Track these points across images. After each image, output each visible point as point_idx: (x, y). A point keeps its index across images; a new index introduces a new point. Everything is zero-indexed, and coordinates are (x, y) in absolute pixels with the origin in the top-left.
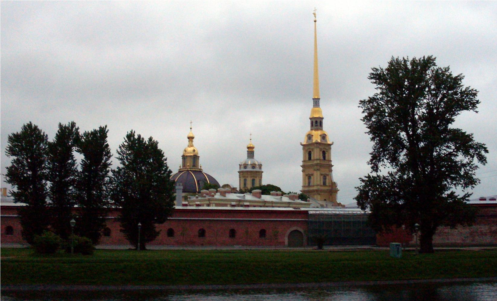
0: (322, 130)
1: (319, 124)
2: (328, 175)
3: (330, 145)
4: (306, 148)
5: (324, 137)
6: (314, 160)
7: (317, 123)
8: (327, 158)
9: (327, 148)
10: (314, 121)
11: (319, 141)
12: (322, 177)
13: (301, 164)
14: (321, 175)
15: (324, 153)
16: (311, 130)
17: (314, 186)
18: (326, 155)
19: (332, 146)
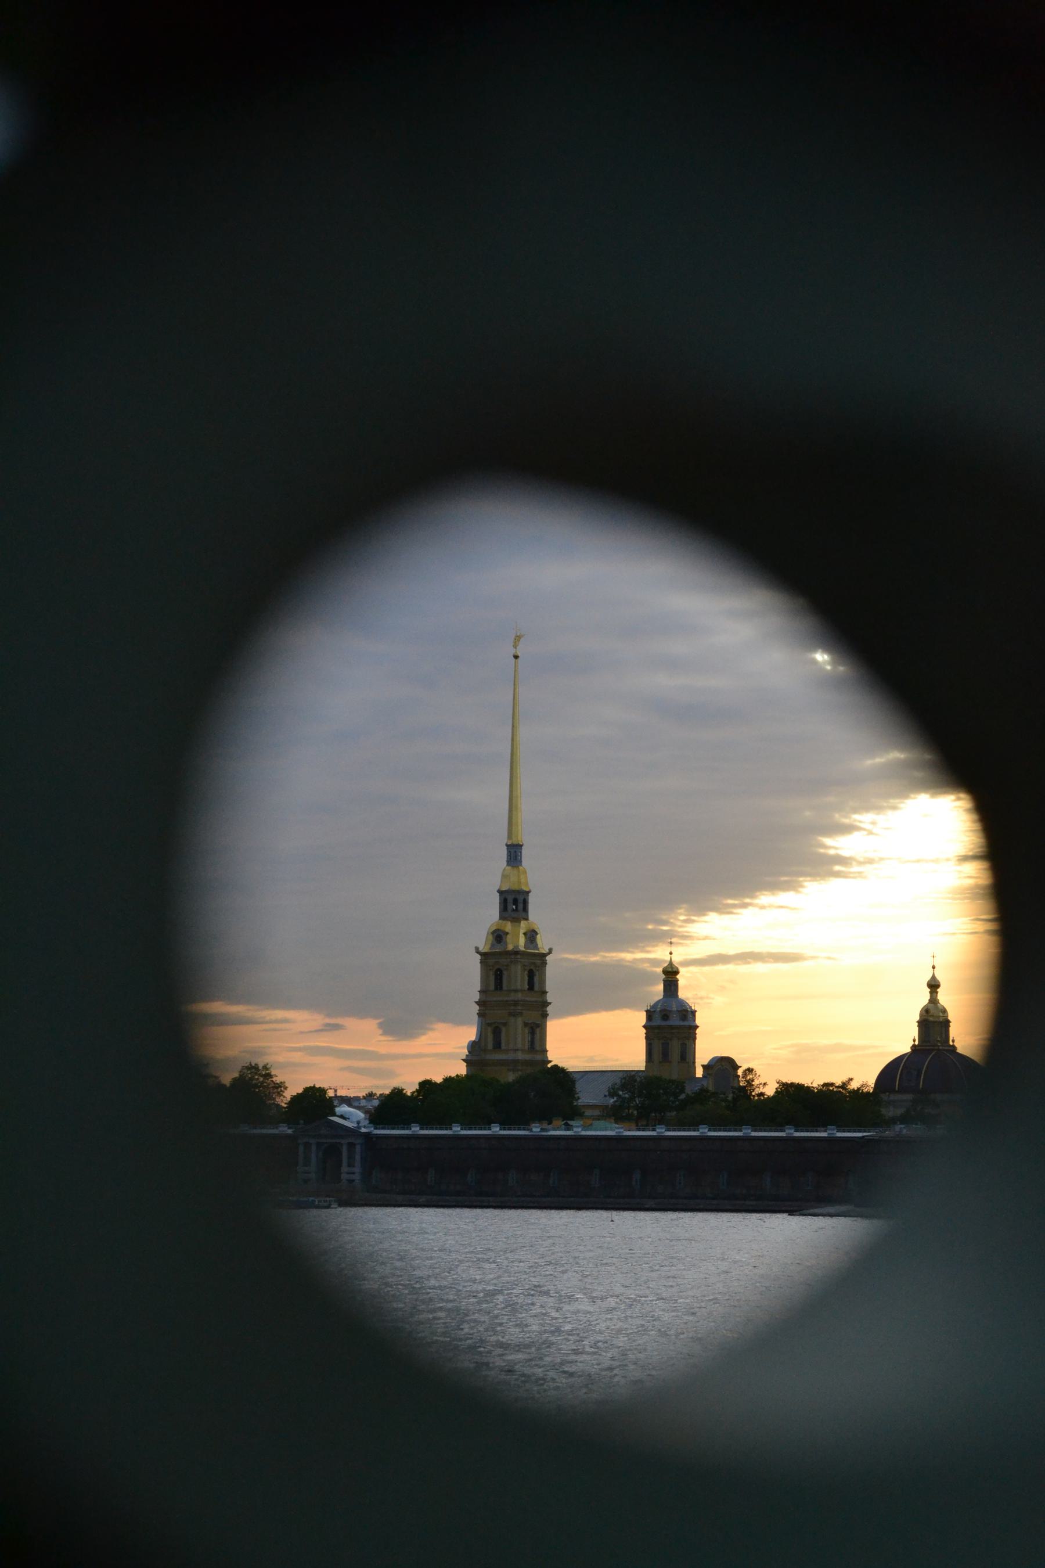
0: (527, 919)
1: (521, 906)
2: (538, 1026)
3: (545, 955)
4: (491, 961)
5: (532, 936)
6: (510, 991)
7: (514, 903)
8: (536, 988)
9: (538, 962)
10: (510, 899)
11: (522, 948)
12: (527, 1030)
13: (477, 997)
14: (526, 1025)
15: (531, 975)
16: (502, 917)
17: (507, 1051)
18: (536, 979)
19: (548, 958)
